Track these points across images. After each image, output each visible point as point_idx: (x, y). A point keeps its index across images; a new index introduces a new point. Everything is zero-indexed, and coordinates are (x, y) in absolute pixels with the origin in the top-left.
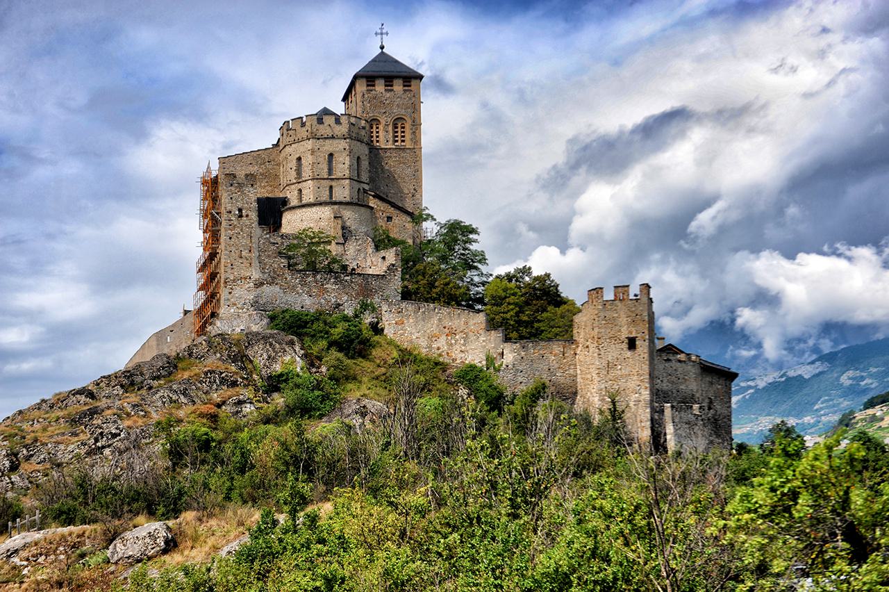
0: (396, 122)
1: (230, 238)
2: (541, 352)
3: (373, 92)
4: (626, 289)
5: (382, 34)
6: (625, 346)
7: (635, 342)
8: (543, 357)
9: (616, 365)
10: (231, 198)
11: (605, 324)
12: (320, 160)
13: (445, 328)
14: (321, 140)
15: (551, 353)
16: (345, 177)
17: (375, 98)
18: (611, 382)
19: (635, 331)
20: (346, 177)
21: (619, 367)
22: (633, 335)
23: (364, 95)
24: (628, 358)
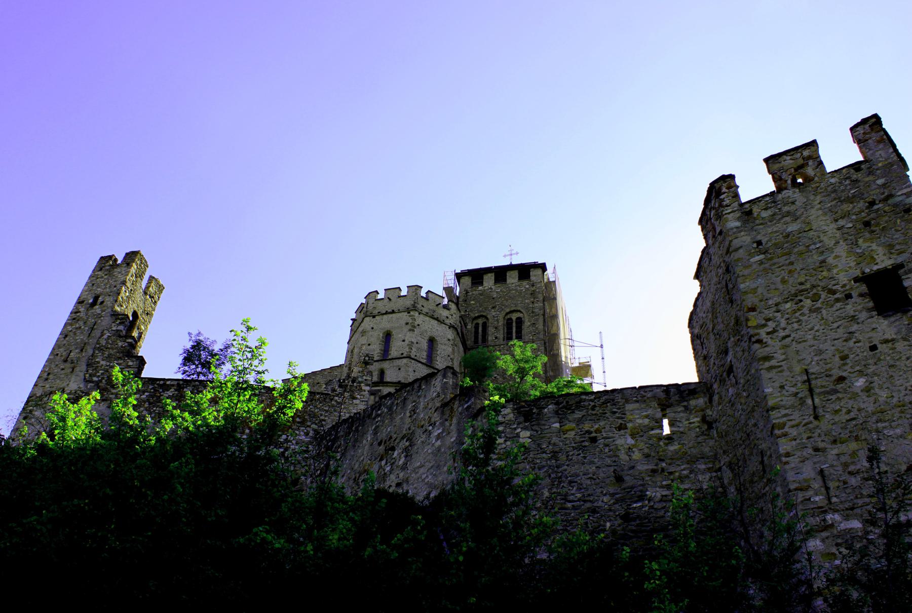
0: (508, 317)
1: (66, 336)
2: (587, 426)
3: (480, 288)
4: (813, 148)
5: (511, 255)
6: (858, 305)
7: (900, 281)
8: (594, 440)
9: (841, 379)
10: (93, 285)
11: (761, 262)
12: (372, 340)
13: (380, 444)
14: (377, 317)
15: (621, 428)
16: (402, 356)
17: (481, 294)
18: (843, 448)
19: (881, 251)
20: (404, 355)
21: (861, 382)
22: (884, 261)
23: (467, 293)
24: (886, 341)
